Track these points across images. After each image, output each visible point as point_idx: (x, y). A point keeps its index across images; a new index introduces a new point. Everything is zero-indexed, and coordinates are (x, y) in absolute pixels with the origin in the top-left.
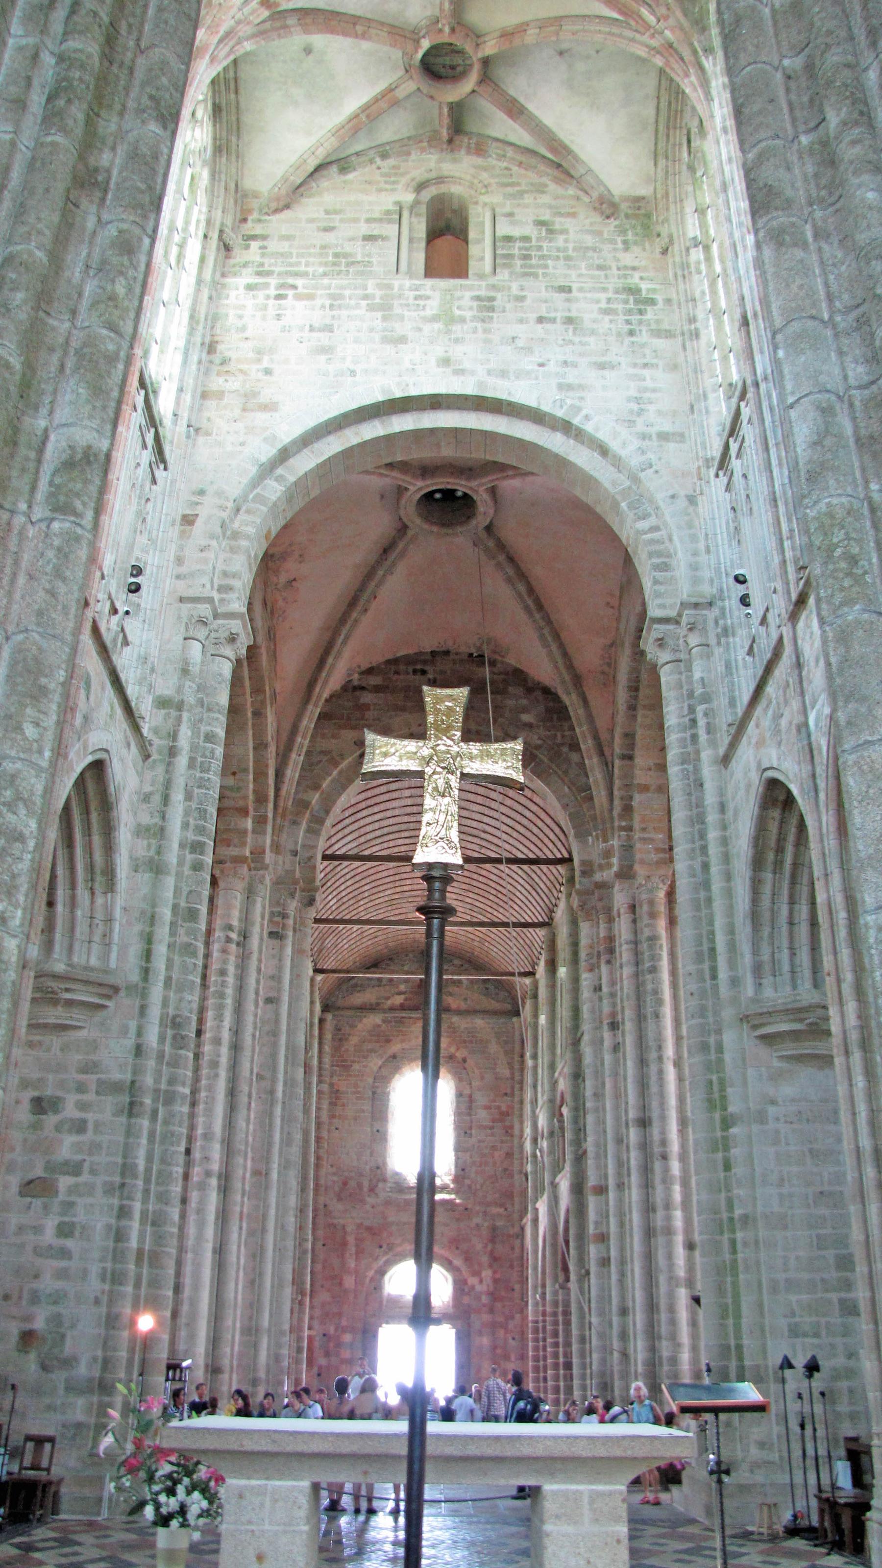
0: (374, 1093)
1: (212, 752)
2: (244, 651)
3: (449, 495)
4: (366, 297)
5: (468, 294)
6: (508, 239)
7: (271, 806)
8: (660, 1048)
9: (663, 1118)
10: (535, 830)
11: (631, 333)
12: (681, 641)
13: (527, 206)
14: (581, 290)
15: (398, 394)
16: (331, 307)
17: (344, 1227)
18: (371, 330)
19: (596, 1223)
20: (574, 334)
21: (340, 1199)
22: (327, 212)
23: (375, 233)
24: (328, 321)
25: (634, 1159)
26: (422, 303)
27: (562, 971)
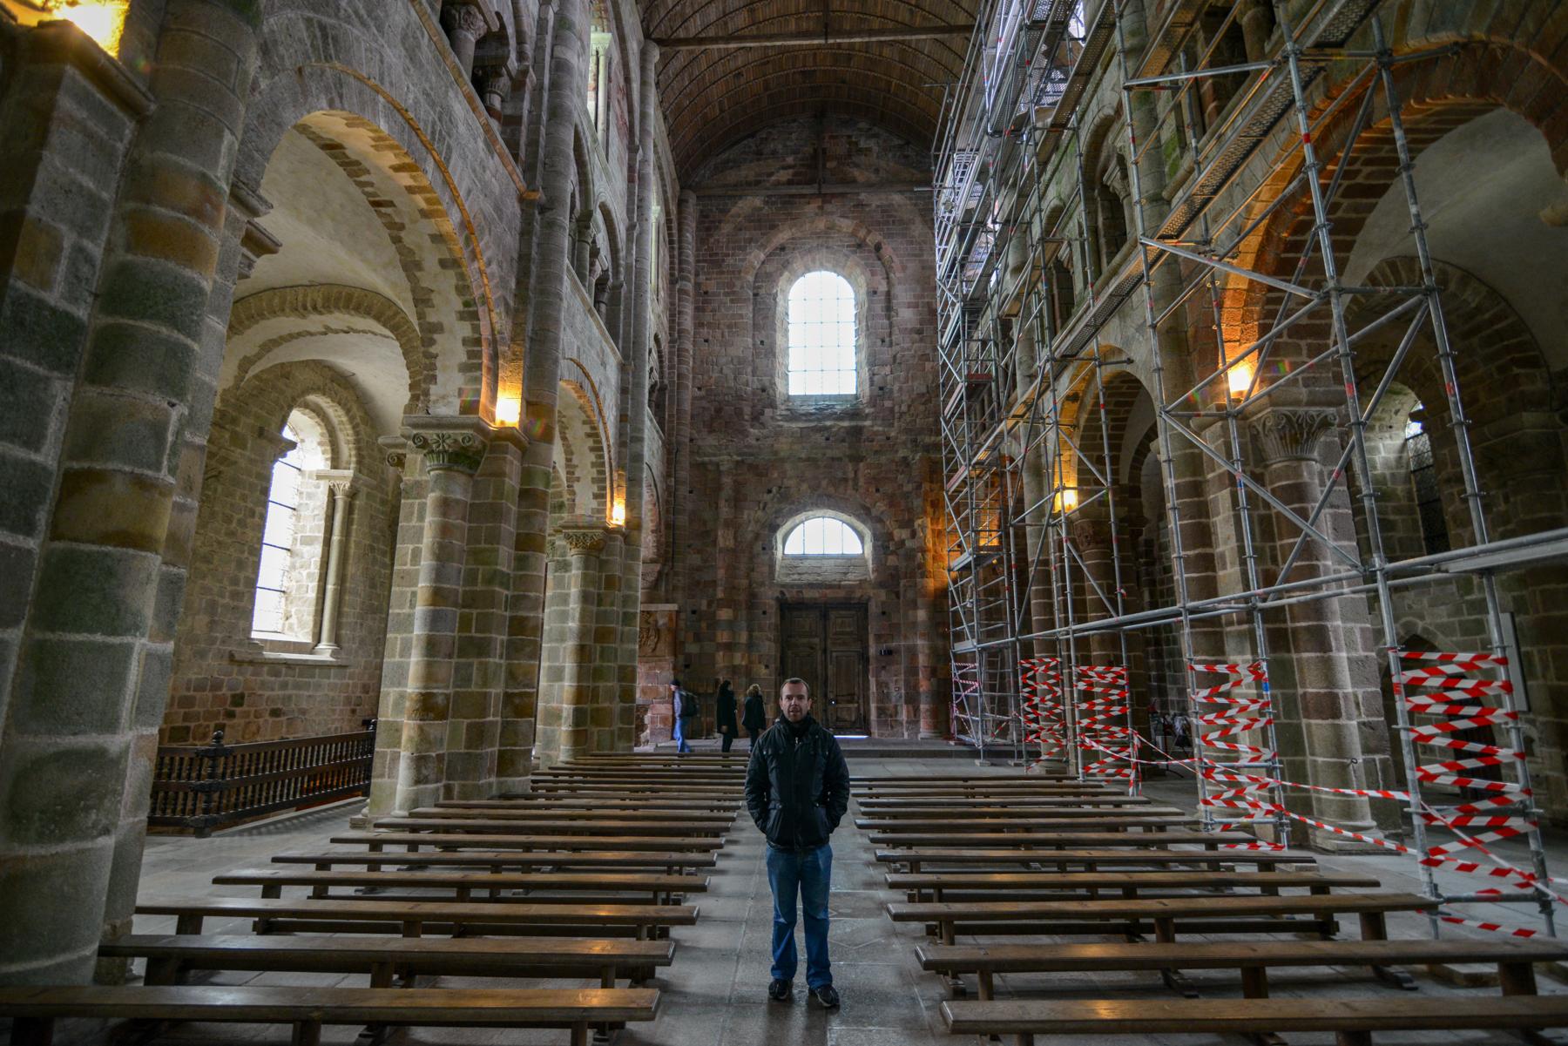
0: (756, 295)
17: (718, 465)
21: (711, 431)
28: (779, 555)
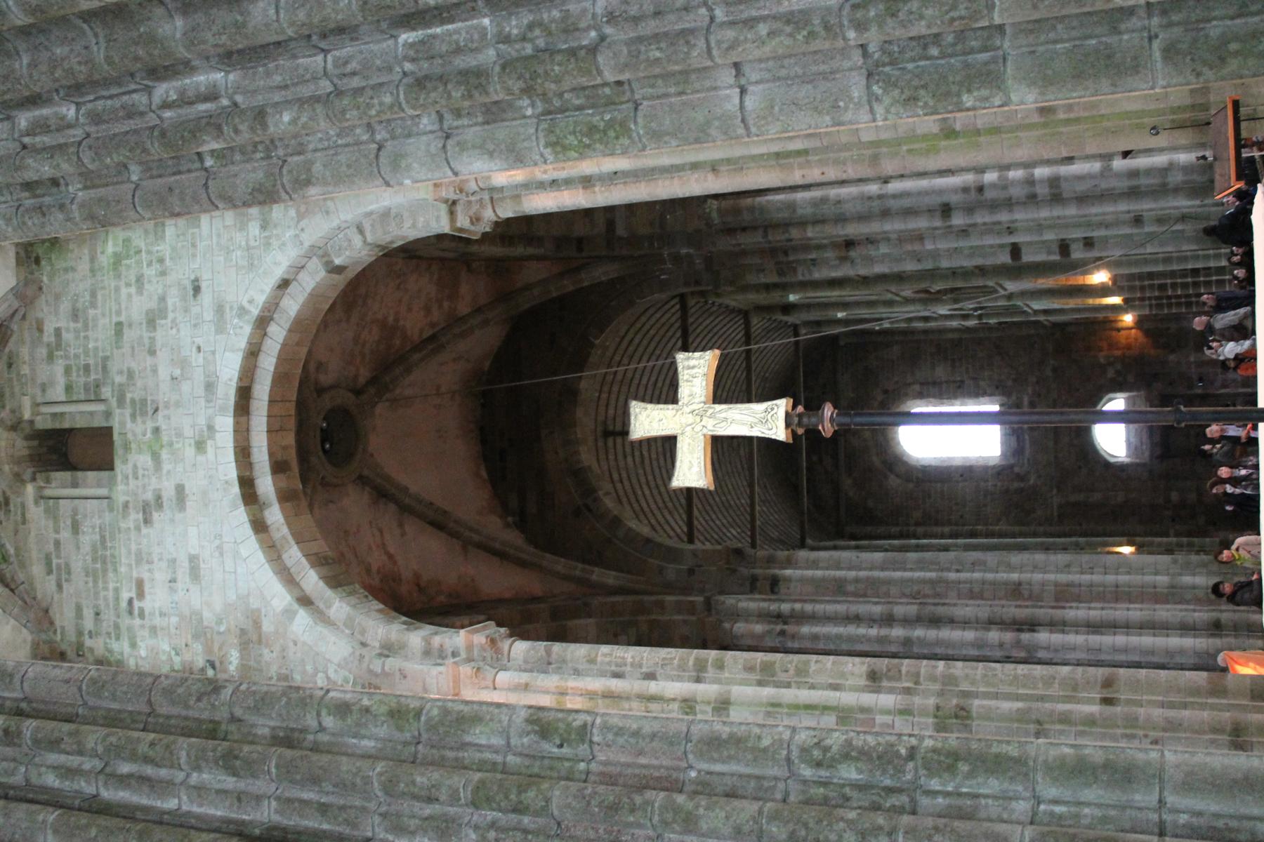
1: (605, 655)
2: (503, 630)
3: (325, 436)
4: (138, 529)
5: (129, 425)
6: (69, 388)
7: (646, 598)
8: (870, 198)
9: (941, 192)
10: (652, 332)
11: (161, 261)
12: (473, 198)
13: (33, 370)
14: (119, 313)
15: (236, 489)
16: (149, 562)
18: (172, 520)
19: (1049, 253)
20: (165, 318)
22: (50, 572)
23: (69, 522)
24: (164, 565)
25: (981, 218)
26: (140, 472)
27: (792, 298)
28: (1127, 460)
